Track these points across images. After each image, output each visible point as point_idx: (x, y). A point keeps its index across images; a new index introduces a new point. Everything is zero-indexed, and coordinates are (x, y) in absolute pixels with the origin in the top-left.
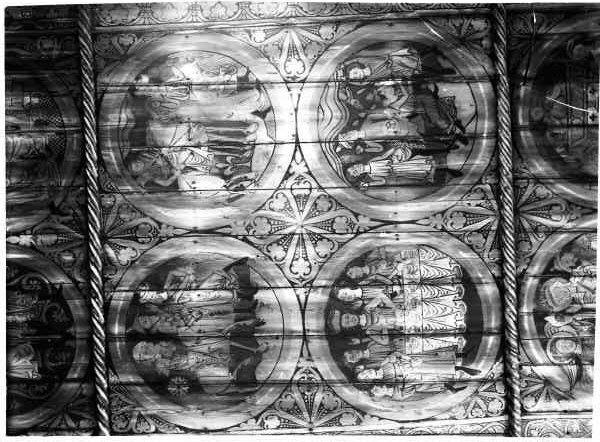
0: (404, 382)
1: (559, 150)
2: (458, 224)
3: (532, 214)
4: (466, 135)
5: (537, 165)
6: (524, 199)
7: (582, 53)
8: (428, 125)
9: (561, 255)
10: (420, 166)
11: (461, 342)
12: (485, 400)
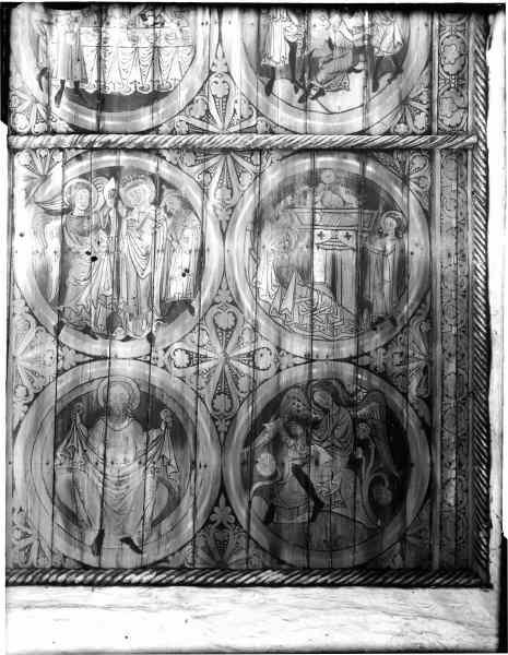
0: (50, 24)
1: (289, 198)
2: (217, 89)
3: (223, 169)
4: (309, 100)
5: (276, 173)
6: (239, 160)
7: (388, 227)
8: (322, 60)
9: (180, 197)
10: (278, 54)
11: (90, 88)
12: (29, 109)
